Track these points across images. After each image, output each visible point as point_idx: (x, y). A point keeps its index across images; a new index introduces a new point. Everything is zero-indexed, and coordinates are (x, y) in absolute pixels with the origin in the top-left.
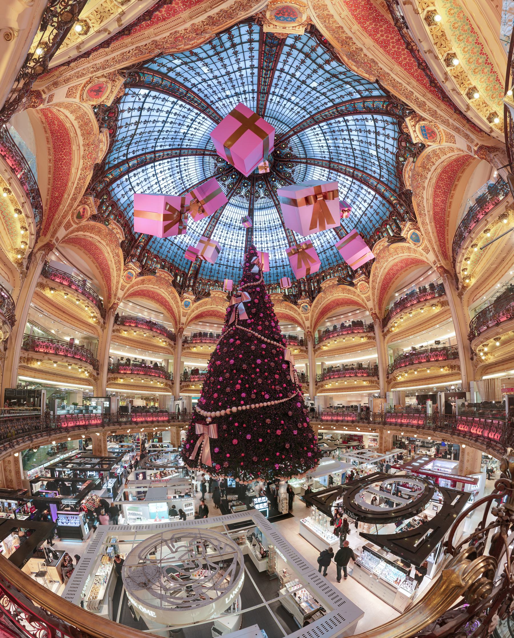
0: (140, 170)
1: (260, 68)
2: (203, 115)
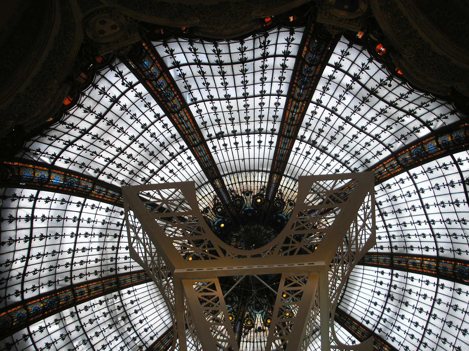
1: (290, 96)
2: (189, 153)
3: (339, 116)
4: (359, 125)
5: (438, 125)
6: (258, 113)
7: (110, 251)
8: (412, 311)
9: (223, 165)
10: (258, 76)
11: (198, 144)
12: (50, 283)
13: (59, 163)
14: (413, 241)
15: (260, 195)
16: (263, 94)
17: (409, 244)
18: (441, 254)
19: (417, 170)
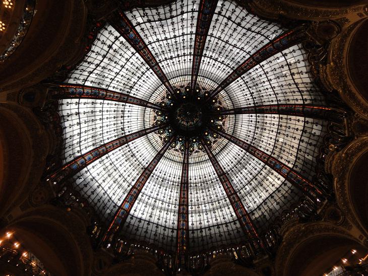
0: (90, 101)
3: (223, 41)
4: (233, 44)
5: (273, 37)
6: (182, 45)
7: (120, 125)
8: (268, 132)
9: (168, 74)
10: (180, 24)
11: (155, 65)
12: (93, 145)
13: (88, 84)
14: (265, 99)
15: (188, 87)
16: (183, 34)
17: (263, 101)
18: (279, 103)
19: (264, 63)
